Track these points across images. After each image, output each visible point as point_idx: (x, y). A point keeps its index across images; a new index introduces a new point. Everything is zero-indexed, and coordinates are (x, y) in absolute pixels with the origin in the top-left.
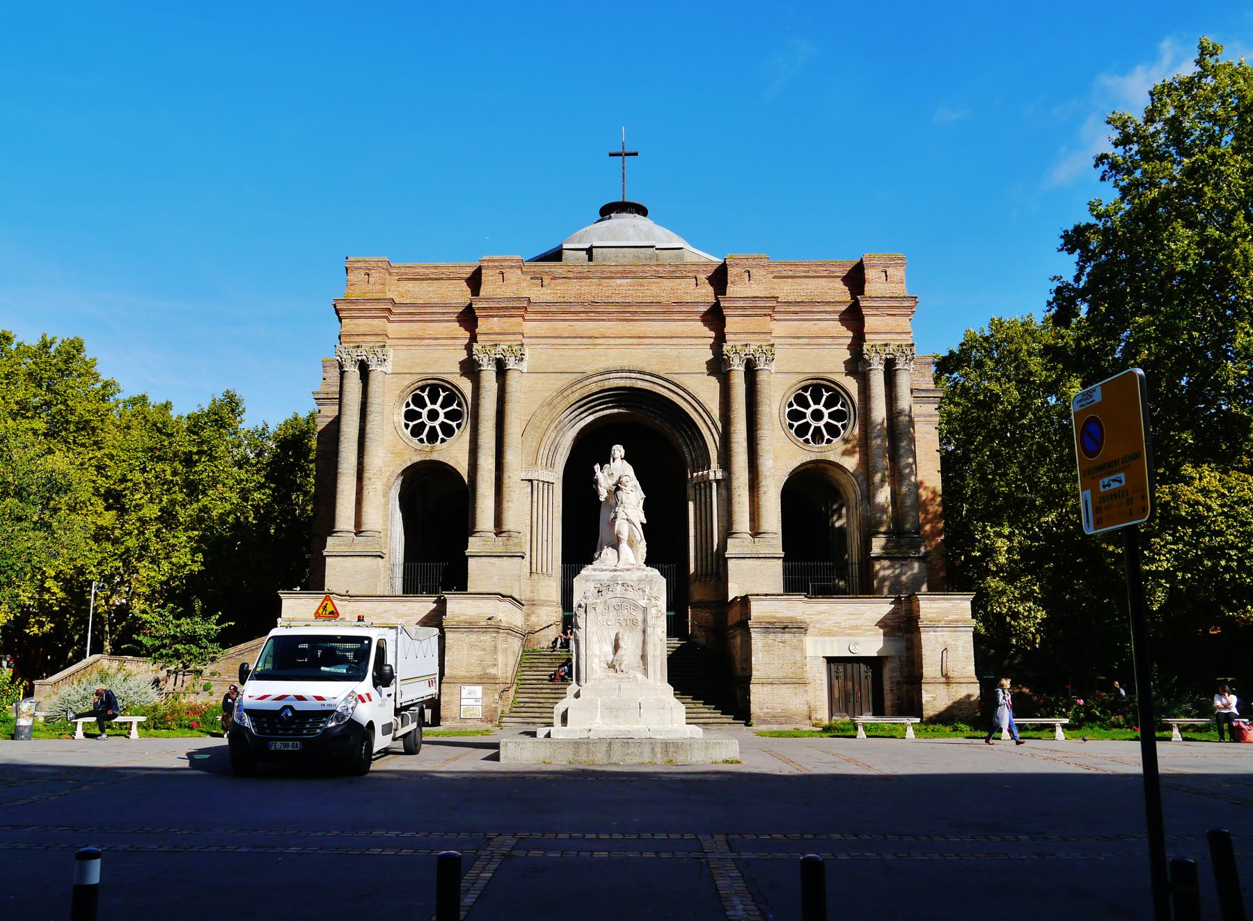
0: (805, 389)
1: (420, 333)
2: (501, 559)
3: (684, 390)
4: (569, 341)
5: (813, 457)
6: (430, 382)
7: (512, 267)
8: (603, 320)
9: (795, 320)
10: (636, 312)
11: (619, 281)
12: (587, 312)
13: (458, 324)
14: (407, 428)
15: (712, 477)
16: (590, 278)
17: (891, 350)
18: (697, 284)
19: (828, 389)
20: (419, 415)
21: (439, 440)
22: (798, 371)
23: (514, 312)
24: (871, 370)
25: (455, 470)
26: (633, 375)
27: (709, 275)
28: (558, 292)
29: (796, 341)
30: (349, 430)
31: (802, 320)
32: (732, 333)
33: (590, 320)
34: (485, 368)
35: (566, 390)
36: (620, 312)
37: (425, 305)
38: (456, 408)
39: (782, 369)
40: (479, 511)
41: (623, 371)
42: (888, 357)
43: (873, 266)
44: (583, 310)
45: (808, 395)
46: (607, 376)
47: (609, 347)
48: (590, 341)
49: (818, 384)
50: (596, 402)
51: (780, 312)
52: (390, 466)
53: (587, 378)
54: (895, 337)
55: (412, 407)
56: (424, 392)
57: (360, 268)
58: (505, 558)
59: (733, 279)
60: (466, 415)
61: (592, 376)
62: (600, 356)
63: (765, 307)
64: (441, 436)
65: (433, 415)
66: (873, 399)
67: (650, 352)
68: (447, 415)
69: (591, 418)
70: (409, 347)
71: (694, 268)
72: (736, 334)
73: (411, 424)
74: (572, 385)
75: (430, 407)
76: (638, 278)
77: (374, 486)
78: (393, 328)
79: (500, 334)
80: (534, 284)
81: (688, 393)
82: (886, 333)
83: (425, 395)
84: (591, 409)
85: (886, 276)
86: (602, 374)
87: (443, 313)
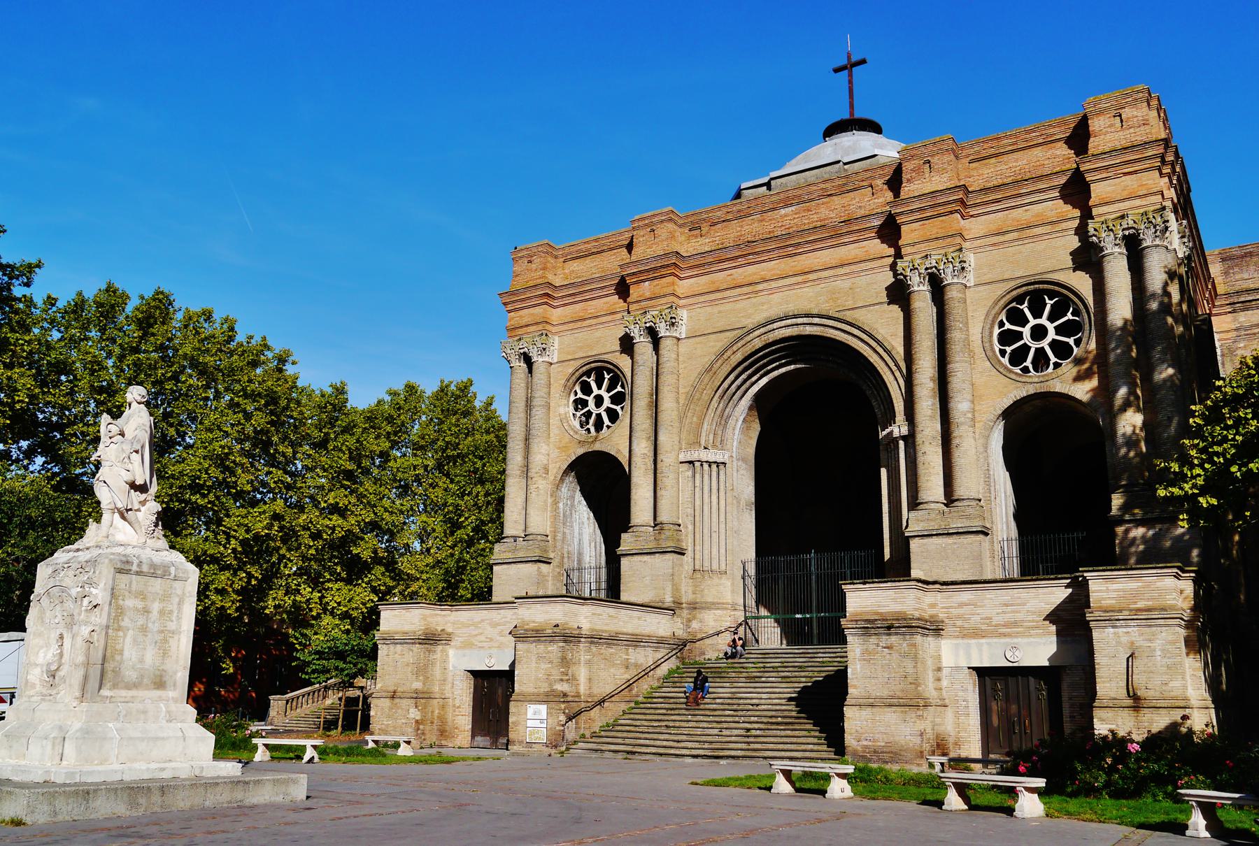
3: (859, 328)
4: (728, 293)
5: (1031, 390)
6: (593, 365)
7: (662, 222)
8: (764, 261)
10: (799, 244)
11: (783, 212)
13: (617, 297)
14: (1003, 356)
16: (751, 215)
17: (1131, 223)
18: (873, 194)
19: (1052, 295)
20: (1019, 336)
21: (1051, 366)
22: (1005, 277)
23: (664, 272)
24: (1104, 256)
26: (800, 320)
27: (887, 178)
29: (1001, 238)
32: (909, 244)
33: (750, 264)
34: (638, 340)
35: (726, 350)
37: (583, 283)
38: (1071, 317)
41: (787, 318)
42: (1127, 233)
43: (1101, 113)
44: (740, 253)
47: (772, 292)
49: (1036, 291)
51: (976, 205)
53: (749, 333)
54: (1138, 202)
55: (1008, 326)
56: (589, 377)
58: (657, 555)
59: (908, 176)
60: (1087, 327)
61: (754, 330)
62: (763, 304)
63: (949, 203)
64: (1053, 359)
65: (1039, 332)
67: (818, 288)
68: (1058, 330)
71: (869, 174)
72: (914, 244)
73: (1009, 349)
75: (1033, 322)
78: (556, 314)
79: (651, 299)
80: (693, 236)
81: (864, 332)
83: (1024, 307)
84: (761, 370)
85: (1122, 121)
86: (764, 325)
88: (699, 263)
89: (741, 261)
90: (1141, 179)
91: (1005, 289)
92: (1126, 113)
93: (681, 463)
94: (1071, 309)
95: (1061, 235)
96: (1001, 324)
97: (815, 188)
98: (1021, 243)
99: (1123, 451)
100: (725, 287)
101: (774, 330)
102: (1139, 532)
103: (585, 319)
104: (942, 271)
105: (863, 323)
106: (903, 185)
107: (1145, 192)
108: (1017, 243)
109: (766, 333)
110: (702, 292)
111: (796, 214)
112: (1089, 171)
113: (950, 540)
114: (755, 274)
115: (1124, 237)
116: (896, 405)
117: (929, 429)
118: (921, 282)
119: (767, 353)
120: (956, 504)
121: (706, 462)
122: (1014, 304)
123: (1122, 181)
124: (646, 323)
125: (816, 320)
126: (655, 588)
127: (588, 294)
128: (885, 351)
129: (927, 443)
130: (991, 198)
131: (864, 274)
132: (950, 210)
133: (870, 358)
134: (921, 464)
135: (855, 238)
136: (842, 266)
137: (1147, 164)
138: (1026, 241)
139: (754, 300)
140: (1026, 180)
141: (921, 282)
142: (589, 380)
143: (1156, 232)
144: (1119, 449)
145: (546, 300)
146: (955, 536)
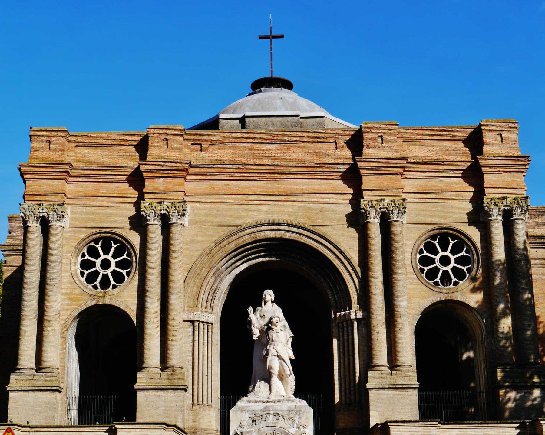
0: (433, 237)
1: (94, 193)
2: (166, 392)
3: (327, 240)
4: (225, 198)
5: (442, 297)
6: (102, 235)
7: (174, 135)
8: (255, 180)
9: (423, 178)
10: (284, 173)
11: (268, 146)
12: (240, 173)
13: (127, 184)
14: (83, 276)
15: (353, 316)
16: (243, 143)
17: (508, 203)
18: (336, 148)
19: (454, 237)
20: (94, 264)
21: (111, 287)
22: (427, 221)
23: (177, 174)
24: (491, 220)
25: (125, 312)
26: (282, 227)
27: (347, 139)
28: (216, 155)
29: (424, 196)
30: (31, 278)
31: (429, 178)
32: (368, 190)
33: (243, 180)
34: (152, 223)
35: (223, 241)
36: (270, 173)
37: (98, 168)
38: (126, 257)
39: (414, 220)
40: (146, 349)
41: (272, 224)
42: (506, 208)
43: (490, 130)
44: (237, 171)
45: (436, 242)
46: (259, 229)
47: (261, 203)
48: (243, 198)
49: (444, 233)
50: (250, 252)
51: (410, 171)
52: (67, 310)
53: (242, 230)
54: (511, 191)
55: (87, 257)
56: (97, 244)
57: (42, 136)
58: (170, 391)
59: (368, 143)
60: (134, 264)
61: (246, 229)
62: (253, 211)
63: (396, 167)
64: (113, 282)
65: (106, 264)
66: (494, 246)
67: (297, 207)
68: (118, 264)
69: (245, 266)
70: (85, 205)
71: (334, 134)
72: (371, 190)
73: (86, 272)
74: (228, 237)
75: (103, 257)
76: (285, 143)
77: (53, 328)
78: (70, 189)
79: (165, 192)
80: (194, 149)
81: (331, 243)
82: (503, 188)
83: (99, 247)
84: (245, 258)
85: (502, 139)
86: (254, 227)
87: (115, 175)
88: (203, 171)
89: (237, 176)
90: (513, 177)
91: (426, 230)
92: (505, 134)
93: (185, 321)
94: (465, 249)
95: (461, 200)
96: (421, 252)
97: (294, 134)
98: (437, 201)
99: (503, 342)
100: (224, 193)
101: (261, 231)
102: (512, 395)
103: (97, 197)
104: (391, 212)
105: (331, 238)
106: (364, 148)
107: (516, 185)
108: (434, 201)
109: (255, 232)
110: (205, 193)
111: (278, 150)
112: (484, 166)
113: (396, 392)
114: (247, 188)
115: (504, 211)
116: (352, 297)
117: (381, 316)
118: (376, 217)
119: (258, 245)
120: (399, 368)
121: (202, 322)
122: (429, 240)
123: (503, 176)
124: (161, 210)
125: (295, 229)
126: (168, 417)
127: (101, 177)
128: (345, 258)
129: (379, 326)
130: (420, 169)
131: (330, 202)
132: (396, 172)
133: (333, 262)
134: (375, 339)
135: (326, 177)
136: (315, 194)
137: (517, 169)
138: (440, 201)
139: (246, 207)
140: (443, 162)
141: (376, 217)
142: (97, 246)
143: (522, 211)
144: (500, 341)
145: (65, 177)
146: (400, 390)
